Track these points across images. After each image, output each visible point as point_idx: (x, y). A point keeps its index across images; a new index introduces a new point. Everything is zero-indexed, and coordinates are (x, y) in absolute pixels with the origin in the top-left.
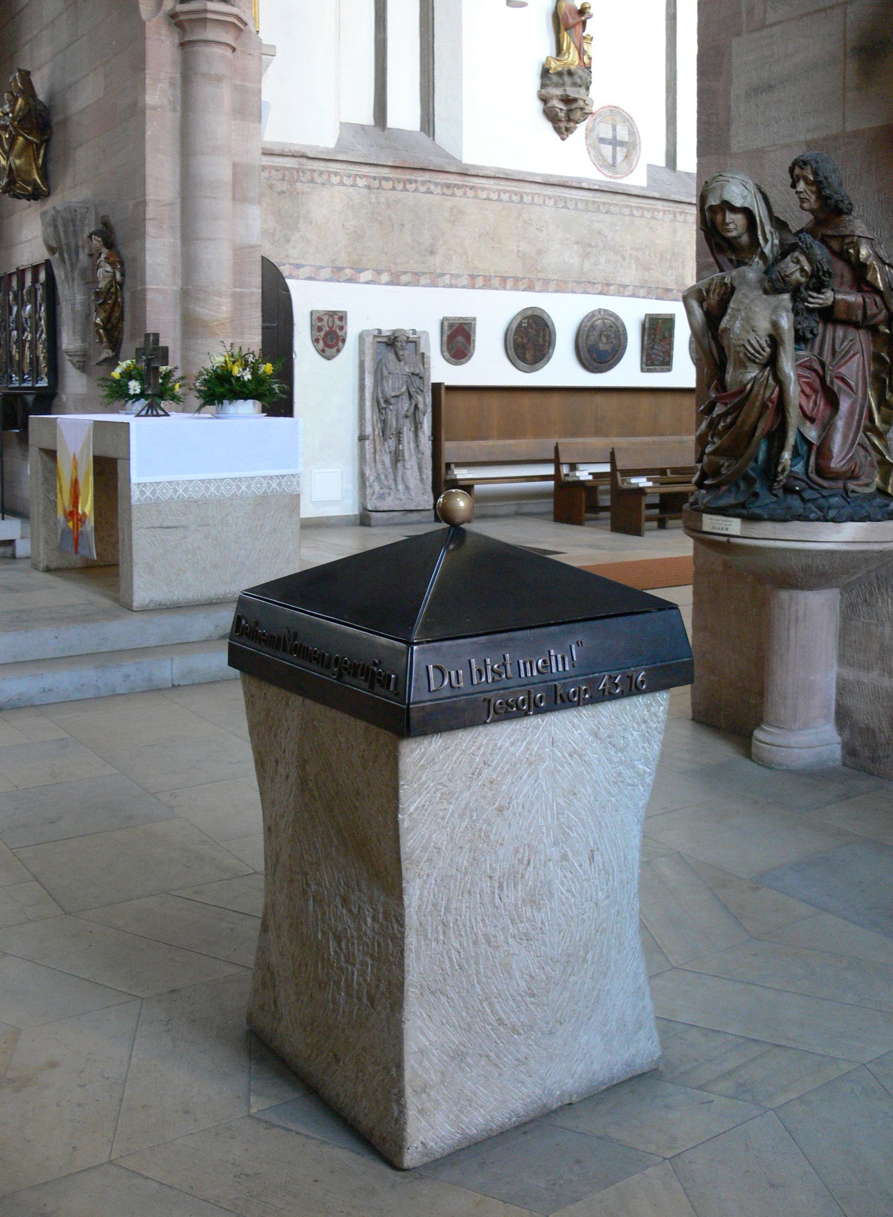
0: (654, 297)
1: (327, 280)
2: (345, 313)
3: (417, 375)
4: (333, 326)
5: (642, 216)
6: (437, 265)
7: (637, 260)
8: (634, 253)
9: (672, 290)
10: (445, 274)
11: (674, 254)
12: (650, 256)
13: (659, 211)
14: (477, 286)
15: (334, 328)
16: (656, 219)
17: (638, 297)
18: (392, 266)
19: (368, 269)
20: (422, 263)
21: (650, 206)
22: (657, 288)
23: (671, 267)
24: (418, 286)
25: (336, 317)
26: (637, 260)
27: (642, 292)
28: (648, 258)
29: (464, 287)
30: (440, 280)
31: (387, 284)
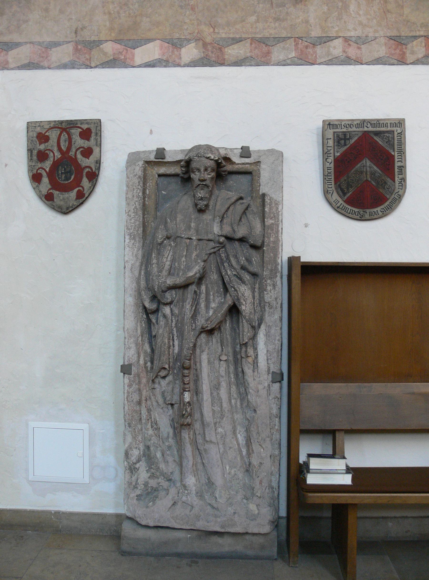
1: (65, 66)
2: (98, 123)
3: (242, 240)
4: (69, 148)
6: (312, 21)
10: (331, 39)
14: (410, 58)
15: (72, 153)
18: (207, 30)
19: (149, 40)
20: (277, 19)
24: (267, 64)
25: (75, 133)
29: (378, 61)
30: (319, 50)
31: (194, 64)
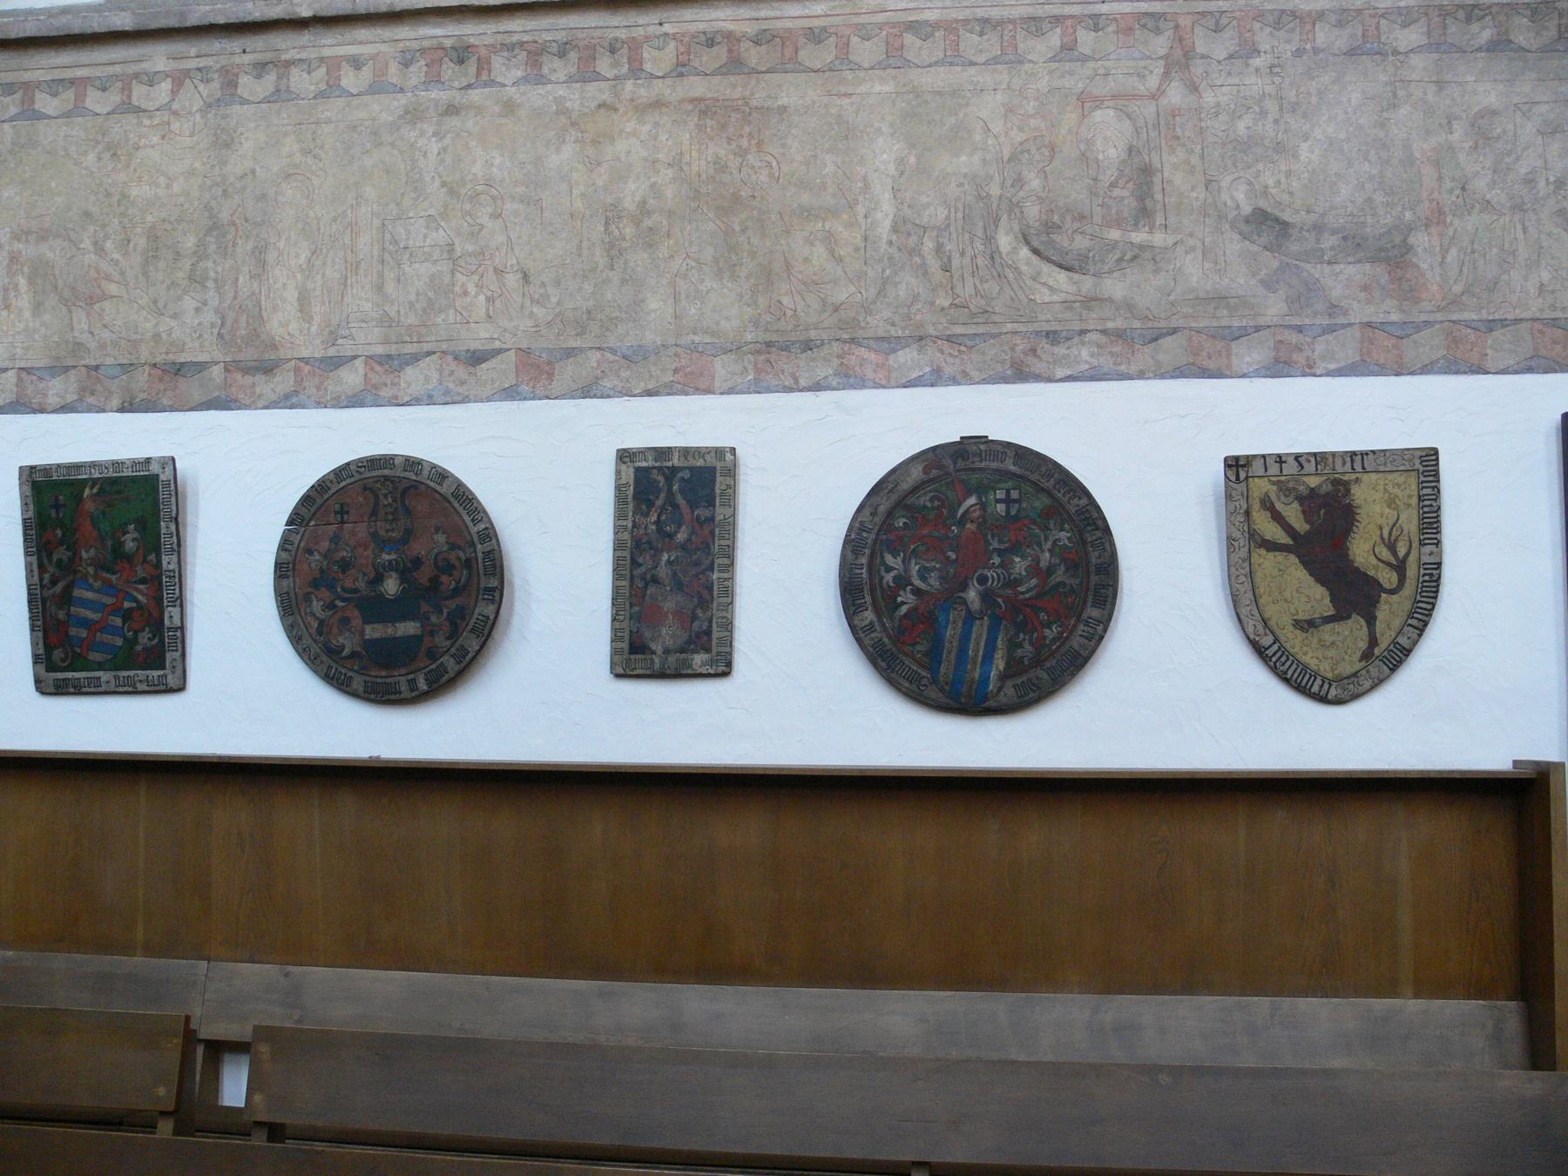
0: (115, 403)
5: (77, 110)
7: (40, 273)
8: (27, 250)
9: (201, 367)
11: (215, 227)
12: (99, 249)
13: (151, 80)
16: (139, 110)
17: (42, 410)
21: (110, 70)
22: (127, 368)
23: (196, 279)
26: (40, 273)
27: (57, 388)
28: (91, 258)
